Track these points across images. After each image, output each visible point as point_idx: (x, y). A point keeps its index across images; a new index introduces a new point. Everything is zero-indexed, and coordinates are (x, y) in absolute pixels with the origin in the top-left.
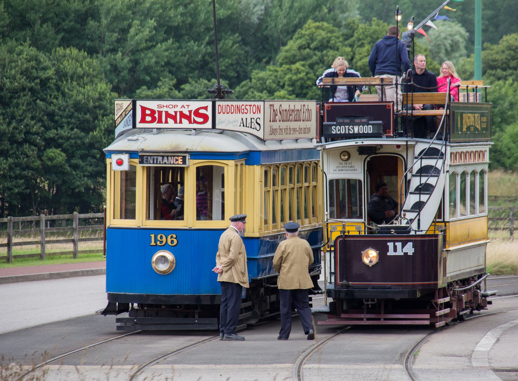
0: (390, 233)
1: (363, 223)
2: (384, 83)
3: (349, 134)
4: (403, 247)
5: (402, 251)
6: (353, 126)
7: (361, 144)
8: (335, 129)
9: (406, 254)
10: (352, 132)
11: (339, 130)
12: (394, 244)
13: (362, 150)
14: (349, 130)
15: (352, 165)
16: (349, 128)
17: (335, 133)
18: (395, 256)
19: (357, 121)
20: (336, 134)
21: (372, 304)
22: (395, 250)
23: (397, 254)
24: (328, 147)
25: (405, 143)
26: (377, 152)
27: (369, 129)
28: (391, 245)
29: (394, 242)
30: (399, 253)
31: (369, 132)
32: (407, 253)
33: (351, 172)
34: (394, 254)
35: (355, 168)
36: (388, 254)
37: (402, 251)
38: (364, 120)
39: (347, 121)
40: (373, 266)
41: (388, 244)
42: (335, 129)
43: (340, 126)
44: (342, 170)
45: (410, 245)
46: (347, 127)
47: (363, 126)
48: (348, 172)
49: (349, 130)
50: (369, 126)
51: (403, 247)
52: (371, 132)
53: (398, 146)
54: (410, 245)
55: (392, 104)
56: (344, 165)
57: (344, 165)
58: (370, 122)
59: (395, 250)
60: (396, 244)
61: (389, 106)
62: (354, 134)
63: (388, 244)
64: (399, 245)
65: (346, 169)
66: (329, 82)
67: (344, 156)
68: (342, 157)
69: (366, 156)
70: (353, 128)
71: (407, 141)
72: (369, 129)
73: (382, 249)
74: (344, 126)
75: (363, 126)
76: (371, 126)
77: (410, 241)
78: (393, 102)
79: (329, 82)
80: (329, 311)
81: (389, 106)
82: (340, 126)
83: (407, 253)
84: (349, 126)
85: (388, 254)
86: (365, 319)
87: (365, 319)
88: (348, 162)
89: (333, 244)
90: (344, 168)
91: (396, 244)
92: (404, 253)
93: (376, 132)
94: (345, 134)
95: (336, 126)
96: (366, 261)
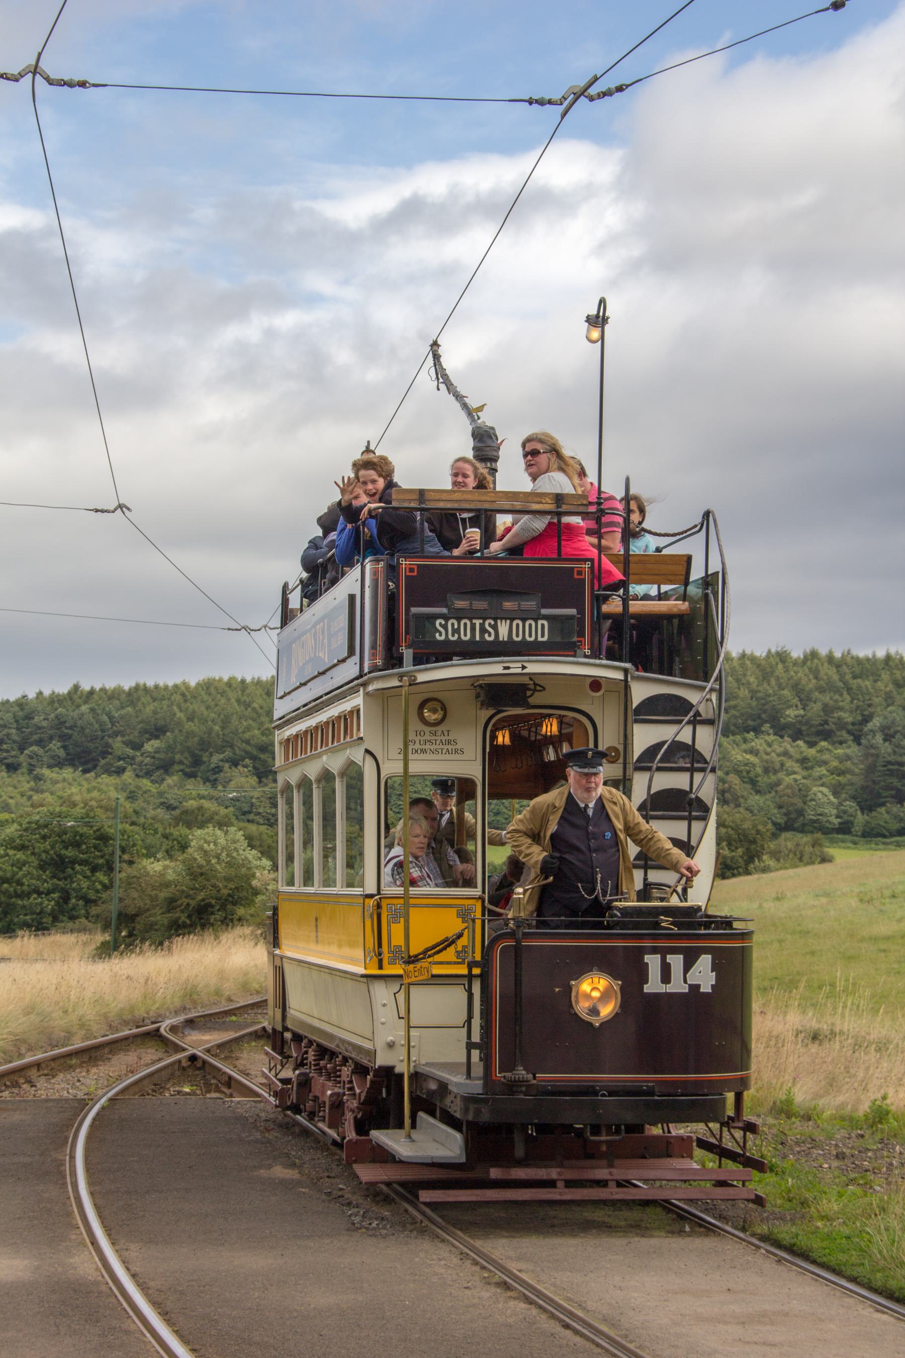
0: (656, 925)
1: (480, 898)
2: (564, 508)
3: (483, 642)
4: (687, 967)
5: (685, 981)
6: (495, 619)
7: (519, 671)
8: (445, 627)
9: (695, 988)
10: (492, 638)
11: (456, 631)
12: (663, 960)
13: (496, 694)
14: (483, 631)
15: (451, 737)
16: (482, 626)
17: (443, 638)
19: (508, 605)
20: (447, 642)
21: (606, 1142)
22: (666, 977)
23: (670, 988)
24: (422, 677)
25: (620, 676)
26: (532, 701)
27: (538, 631)
28: (653, 962)
29: (664, 952)
30: (677, 986)
31: (540, 639)
32: (698, 986)
33: (448, 756)
34: (662, 989)
35: (458, 747)
36: (647, 989)
37: (685, 981)
38: (530, 604)
39: (480, 604)
40: (602, 1024)
41: (647, 958)
42: (445, 627)
43: (459, 619)
44: (424, 751)
45: (705, 961)
46: (477, 622)
47: (524, 620)
48: (440, 756)
49: (483, 631)
50: (540, 622)
51: (687, 967)
52: (545, 638)
53: (596, 684)
54: (705, 961)
55: (587, 565)
56: (427, 737)
57: (427, 737)
58: (544, 611)
59: (666, 977)
60: (670, 958)
61: (580, 573)
62: (497, 641)
63: (647, 958)
64: (676, 961)
65: (433, 747)
66: (410, 501)
67: (434, 711)
68: (426, 713)
69: (491, 712)
70: (495, 627)
71: (626, 671)
72: (538, 631)
73: (629, 973)
74: (471, 619)
75: (524, 620)
76: (545, 623)
77: (706, 951)
78: (592, 560)
79: (410, 501)
80: (463, 1160)
81: (580, 573)
82: (459, 619)
83: (698, 986)
84: (485, 619)
85: (647, 989)
86: (560, 1184)
87: (560, 1184)
88: (439, 729)
89: (478, 957)
90: (428, 746)
91: (670, 958)
92: (690, 986)
93: (558, 639)
94: (472, 641)
95: (447, 618)
96: (582, 1007)
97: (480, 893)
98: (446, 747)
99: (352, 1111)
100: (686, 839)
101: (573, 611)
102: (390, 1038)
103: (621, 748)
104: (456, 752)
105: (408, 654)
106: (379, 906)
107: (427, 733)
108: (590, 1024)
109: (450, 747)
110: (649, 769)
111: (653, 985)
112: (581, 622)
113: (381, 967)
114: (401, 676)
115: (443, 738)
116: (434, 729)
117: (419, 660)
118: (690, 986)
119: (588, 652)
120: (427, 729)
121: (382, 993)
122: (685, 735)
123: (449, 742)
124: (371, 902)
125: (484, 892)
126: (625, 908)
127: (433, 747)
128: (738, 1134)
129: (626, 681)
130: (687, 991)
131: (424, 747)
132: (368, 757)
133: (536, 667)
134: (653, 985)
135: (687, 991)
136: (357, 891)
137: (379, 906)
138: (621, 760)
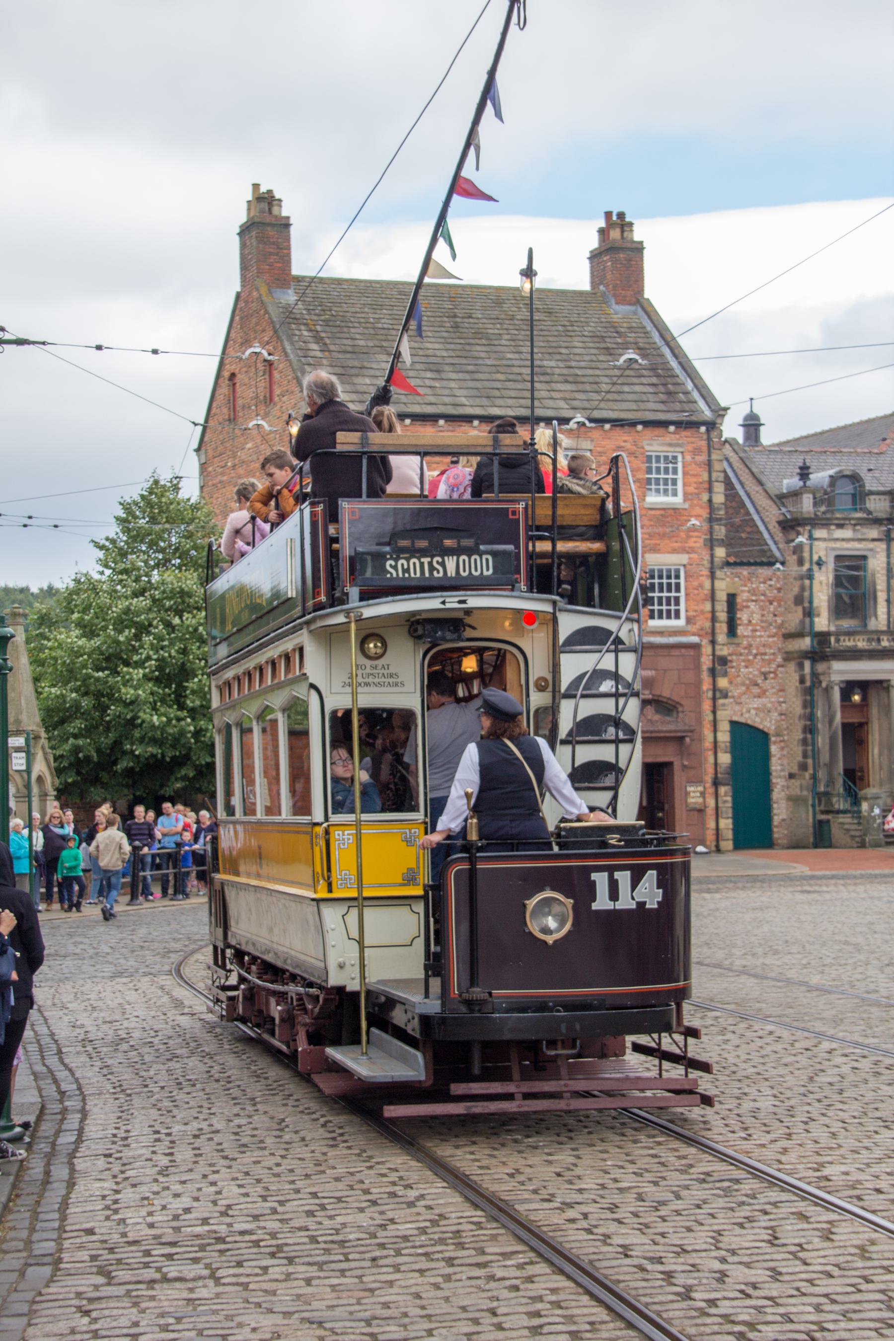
0: (604, 844)
4: (634, 886)
5: (633, 898)
18: (615, 911)
22: (614, 895)
23: (620, 905)
28: (600, 879)
30: (626, 902)
32: (645, 903)
33: (389, 689)
35: (399, 680)
39: (422, 544)
48: (383, 689)
51: (634, 886)
59: (614, 895)
60: (617, 875)
61: (514, 513)
64: (624, 878)
65: (376, 680)
81: (514, 513)
83: (645, 903)
90: (370, 680)
91: (617, 875)
92: (638, 903)
97: (422, 817)
98: (387, 680)
99: (305, 1025)
100: (614, 761)
101: (510, 547)
102: (341, 960)
103: (549, 677)
104: (397, 685)
105: (354, 592)
106: (327, 832)
107: (368, 667)
108: (545, 942)
109: (391, 680)
110: (574, 696)
111: (602, 902)
112: (518, 555)
113: (330, 891)
114: (347, 613)
115: (383, 671)
116: (375, 663)
117: (365, 596)
118: (638, 903)
119: (523, 587)
120: (368, 663)
121: (332, 915)
122: (607, 662)
123: (391, 676)
124: (319, 830)
125: (426, 815)
126: (572, 828)
127: (376, 680)
128: (679, 1038)
129: (554, 614)
130: (634, 907)
131: (366, 680)
132: (313, 693)
133: (474, 601)
134: (602, 902)
135: (634, 907)
136: (305, 819)
137: (327, 832)
138: (550, 688)
